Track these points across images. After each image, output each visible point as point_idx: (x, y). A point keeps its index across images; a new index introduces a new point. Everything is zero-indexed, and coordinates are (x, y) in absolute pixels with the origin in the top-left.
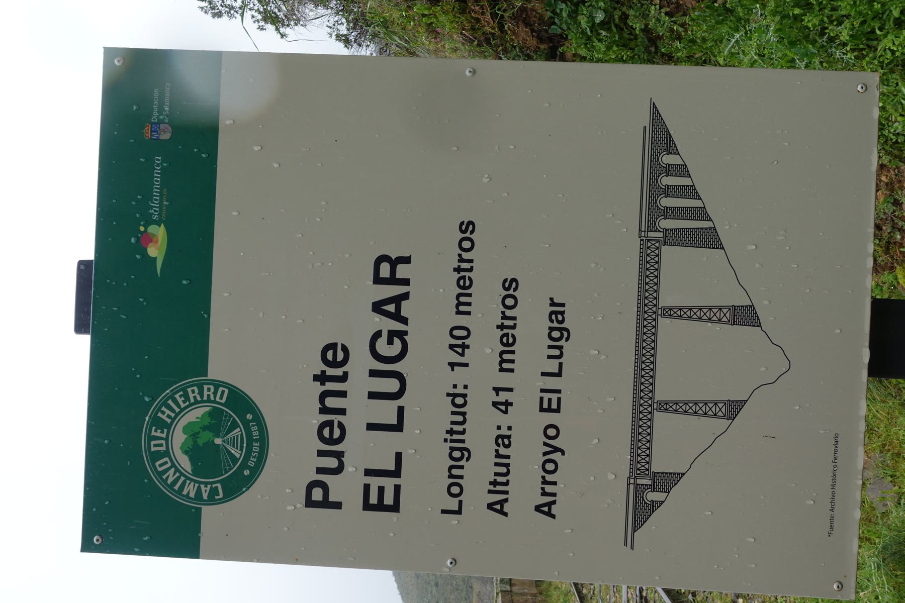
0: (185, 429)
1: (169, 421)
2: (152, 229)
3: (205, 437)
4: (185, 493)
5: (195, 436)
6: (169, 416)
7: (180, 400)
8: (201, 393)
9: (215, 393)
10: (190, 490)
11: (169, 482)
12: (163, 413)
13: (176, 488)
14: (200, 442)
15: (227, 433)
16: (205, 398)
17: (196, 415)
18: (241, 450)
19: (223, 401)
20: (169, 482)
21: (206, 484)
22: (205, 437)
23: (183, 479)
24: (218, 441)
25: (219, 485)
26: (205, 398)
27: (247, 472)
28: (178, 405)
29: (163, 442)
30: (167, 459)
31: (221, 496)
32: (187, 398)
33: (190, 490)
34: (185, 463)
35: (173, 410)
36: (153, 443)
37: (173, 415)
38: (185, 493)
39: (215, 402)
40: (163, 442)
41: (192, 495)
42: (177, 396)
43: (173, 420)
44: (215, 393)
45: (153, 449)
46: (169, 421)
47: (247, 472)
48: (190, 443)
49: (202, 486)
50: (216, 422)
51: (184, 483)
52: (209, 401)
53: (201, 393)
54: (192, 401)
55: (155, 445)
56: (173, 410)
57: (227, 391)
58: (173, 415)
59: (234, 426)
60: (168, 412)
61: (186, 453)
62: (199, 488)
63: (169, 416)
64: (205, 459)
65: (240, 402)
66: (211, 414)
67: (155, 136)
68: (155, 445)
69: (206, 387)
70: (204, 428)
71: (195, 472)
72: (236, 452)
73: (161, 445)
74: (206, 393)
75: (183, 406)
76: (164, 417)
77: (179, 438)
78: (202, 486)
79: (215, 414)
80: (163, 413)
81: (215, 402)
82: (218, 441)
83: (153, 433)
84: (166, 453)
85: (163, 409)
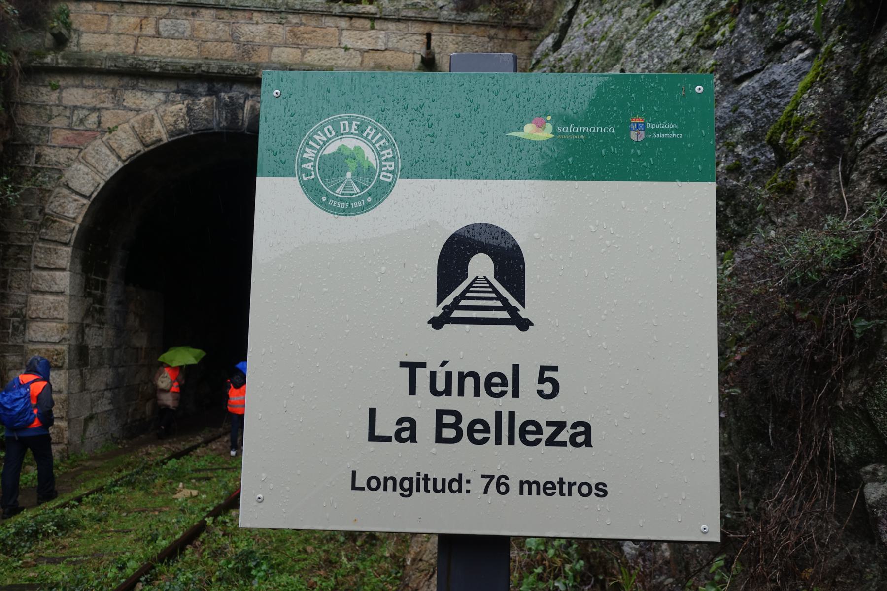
0: (358, 148)
1: (364, 135)
2: (549, 127)
3: (352, 165)
4: (307, 149)
6: (368, 134)
7: (381, 143)
8: (386, 160)
9: (388, 171)
10: (309, 154)
11: (315, 137)
12: (371, 130)
13: (311, 143)
15: (356, 183)
16: (384, 163)
17: (370, 156)
18: (343, 194)
19: (381, 178)
20: (315, 137)
21: (314, 166)
22: (352, 165)
23: (318, 147)
24: (349, 175)
25: (313, 177)
26: (384, 163)
27: (324, 199)
28: (376, 143)
29: (347, 131)
30: (334, 134)
31: (305, 179)
32: (384, 148)
33: (309, 154)
34: (331, 149)
35: (372, 139)
36: (347, 123)
37: (369, 138)
38: (307, 149)
39: (381, 171)
40: (347, 131)
41: (305, 155)
42: (384, 141)
43: (366, 138)
44: (388, 171)
45: (341, 123)
46: (364, 135)
47: (324, 199)
48: (347, 153)
49: (312, 163)
50: (365, 173)
51: (316, 149)
53: (386, 160)
54: (382, 153)
55: (344, 124)
56: (372, 139)
57: (390, 180)
58: (369, 138)
59: (362, 188)
60: (372, 133)
61: (339, 150)
62: (310, 161)
63: (368, 134)
64: (333, 166)
67: (634, 127)
68: (344, 124)
69: (392, 163)
72: (340, 190)
73: (345, 130)
74: (387, 164)
75: (377, 145)
76: (367, 131)
77: (351, 143)
78: (312, 163)
79: (371, 172)
80: (371, 130)
81: (381, 171)
82: (349, 175)
83: (354, 123)
84: (338, 134)
85: (374, 130)
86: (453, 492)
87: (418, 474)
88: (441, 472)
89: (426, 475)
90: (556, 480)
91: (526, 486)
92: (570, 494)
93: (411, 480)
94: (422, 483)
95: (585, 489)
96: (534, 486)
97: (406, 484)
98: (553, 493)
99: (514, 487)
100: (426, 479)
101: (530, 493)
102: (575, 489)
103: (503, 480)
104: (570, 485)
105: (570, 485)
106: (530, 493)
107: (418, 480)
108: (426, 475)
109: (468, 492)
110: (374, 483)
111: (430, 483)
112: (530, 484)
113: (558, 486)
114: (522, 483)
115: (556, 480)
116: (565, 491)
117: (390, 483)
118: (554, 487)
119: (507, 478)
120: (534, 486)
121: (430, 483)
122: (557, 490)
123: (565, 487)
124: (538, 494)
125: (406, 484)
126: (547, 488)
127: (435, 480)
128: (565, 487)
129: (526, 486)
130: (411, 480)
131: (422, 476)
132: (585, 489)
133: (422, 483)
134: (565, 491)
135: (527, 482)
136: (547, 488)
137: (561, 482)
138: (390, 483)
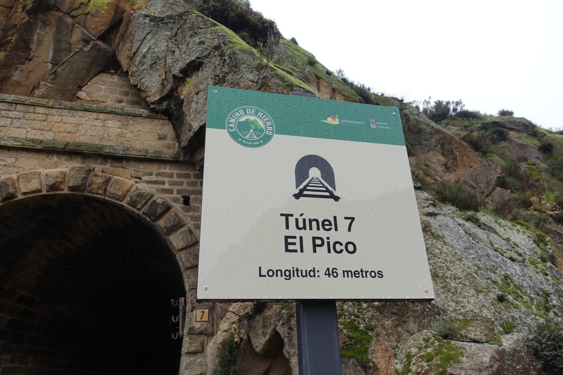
3: (253, 127)
5: (253, 123)
14: (251, 125)
17: (261, 124)
22: (253, 127)
34: (243, 119)
50: (259, 130)
52: (266, 128)
61: (246, 120)
65: (266, 139)
66: (262, 129)
70: (256, 127)
71: (239, 123)
77: (252, 118)
79: (262, 130)
84: (246, 113)
86: (312, 277)
87: (293, 268)
88: (305, 267)
89: (297, 268)
90: (359, 270)
91: (346, 273)
92: (366, 277)
93: (290, 271)
94: (295, 272)
95: (373, 274)
96: (350, 273)
97: (287, 273)
98: (359, 276)
99: (340, 272)
100: (297, 270)
101: (348, 277)
102: (368, 274)
103: (334, 270)
104: (366, 272)
105: (366, 272)
106: (348, 277)
107: (293, 271)
108: (297, 268)
109: (318, 276)
110: (271, 273)
111: (300, 272)
112: (348, 272)
113: (360, 273)
114: (344, 272)
115: (359, 270)
116: (364, 275)
117: (279, 273)
118: (359, 274)
119: (336, 269)
120: (350, 273)
121: (300, 272)
122: (361, 275)
123: (364, 273)
124: (352, 277)
125: (287, 273)
126: (356, 274)
127: (302, 271)
128: (364, 273)
129: (346, 273)
130: (290, 271)
131: (295, 269)
132: (373, 274)
133: (295, 272)
134: (364, 275)
135: (346, 271)
136: (356, 274)
137: (362, 271)
138: (279, 273)
